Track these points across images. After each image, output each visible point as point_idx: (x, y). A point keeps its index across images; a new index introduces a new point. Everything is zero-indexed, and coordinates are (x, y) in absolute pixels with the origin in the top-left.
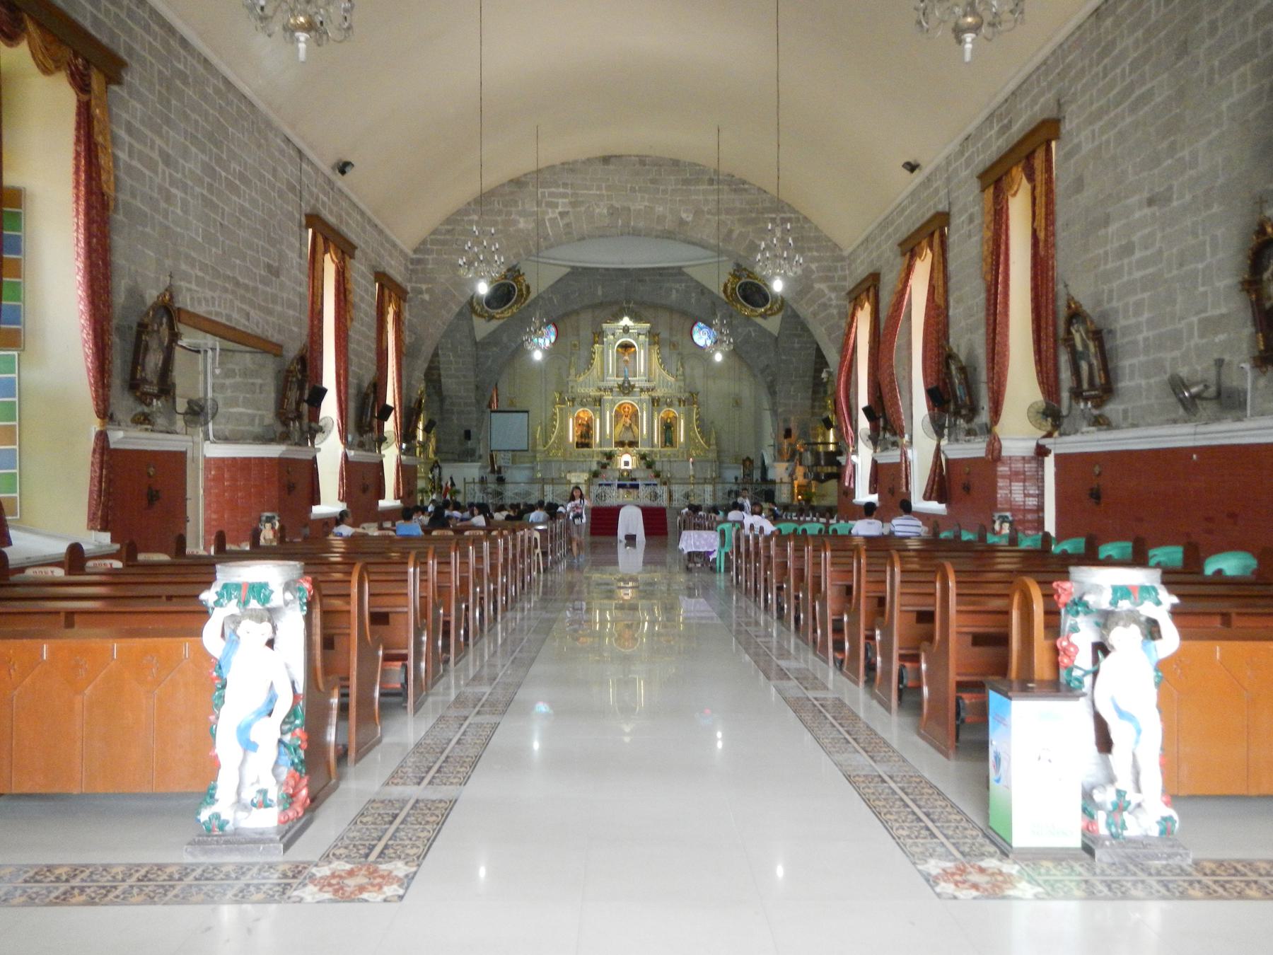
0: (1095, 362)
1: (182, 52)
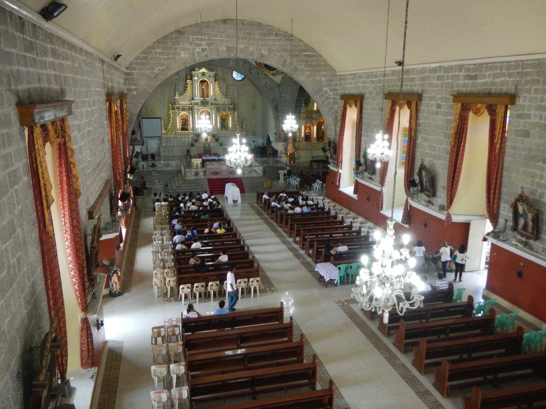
0: (530, 224)
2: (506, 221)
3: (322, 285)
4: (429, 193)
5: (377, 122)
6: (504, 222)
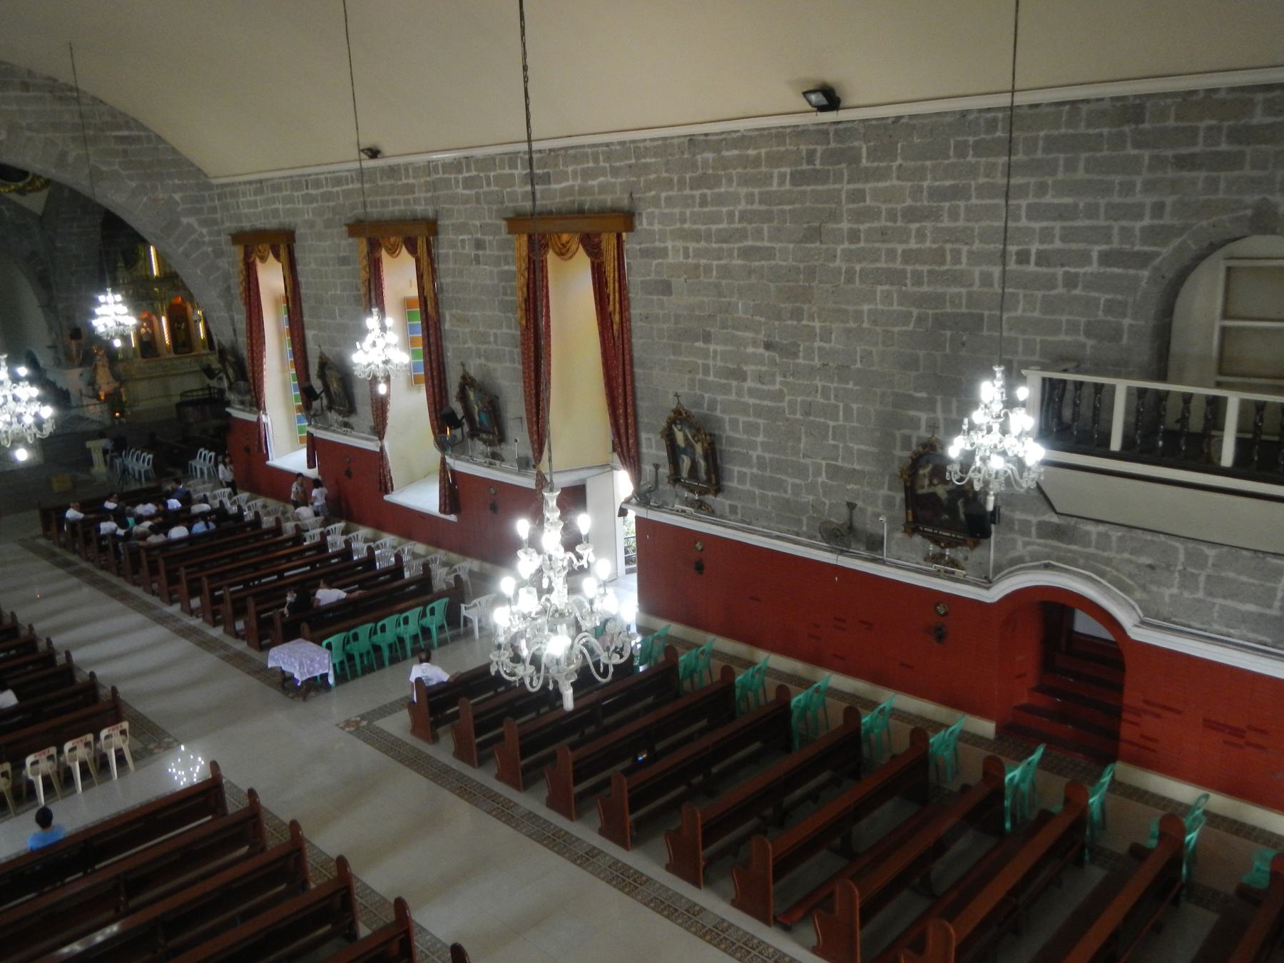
0: (702, 463)
2: (657, 466)
3: (293, 698)
4: (491, 437)
5: (339, 292)
6: (653, 468)
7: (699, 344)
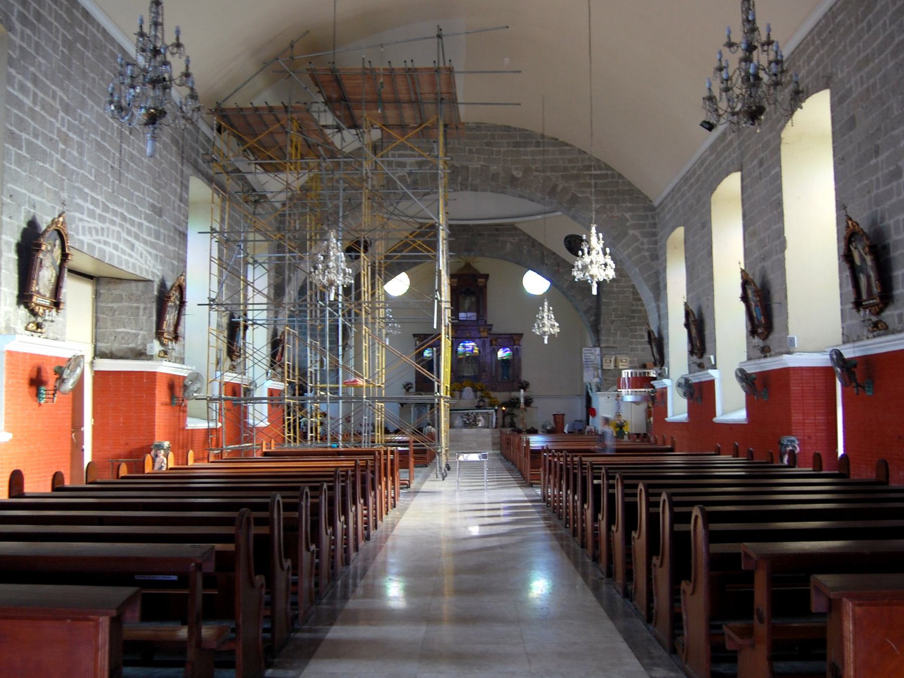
0: (872, 274)
1: (84, 21)
7: (873, 162)
